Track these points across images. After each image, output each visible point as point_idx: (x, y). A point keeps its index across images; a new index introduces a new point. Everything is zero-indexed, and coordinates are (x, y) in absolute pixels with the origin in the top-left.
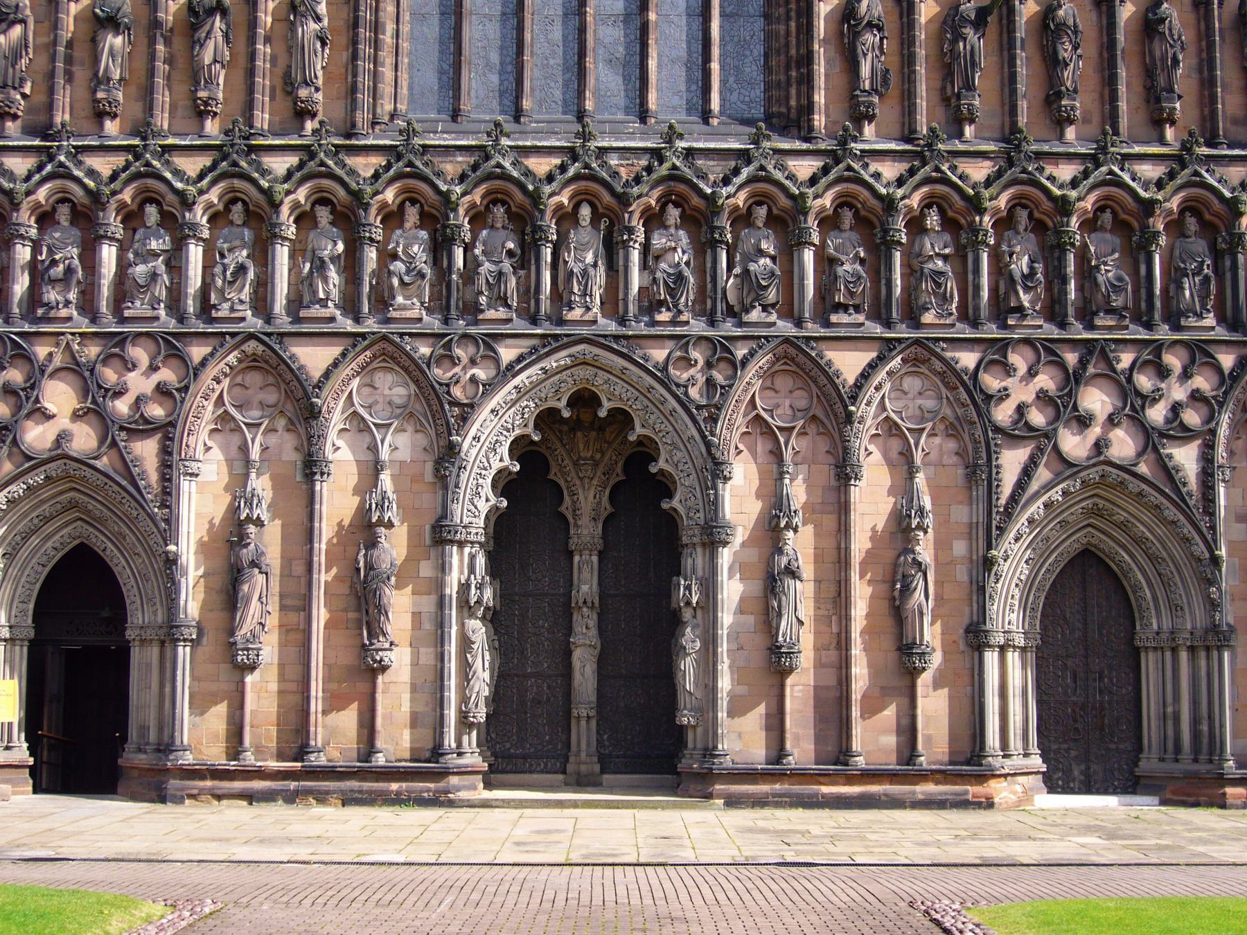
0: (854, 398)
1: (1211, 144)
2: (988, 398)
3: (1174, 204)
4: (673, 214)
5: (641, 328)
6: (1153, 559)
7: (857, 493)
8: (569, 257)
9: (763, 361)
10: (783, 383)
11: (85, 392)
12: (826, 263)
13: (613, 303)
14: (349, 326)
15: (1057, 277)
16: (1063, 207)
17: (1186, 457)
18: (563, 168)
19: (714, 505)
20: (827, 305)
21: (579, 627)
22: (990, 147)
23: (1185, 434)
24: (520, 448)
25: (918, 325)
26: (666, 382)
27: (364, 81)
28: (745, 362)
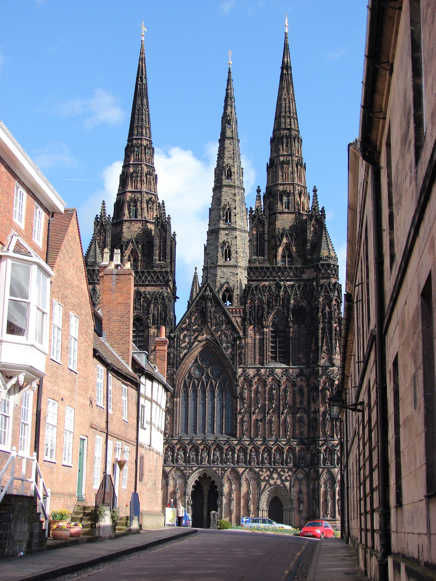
0: (242, 476)
1: (293, 439)
2: (260, 476)
3: (287, 448)
4: (217, 449)
5: (212, 465)
7: (242, 488)
8: (203, 455)
9: (229, 470)
10: (232, 473)
12: (238, 456)
13: (209, 462)
14: (172, 465)
15: (270, 458)
16: (271, 448)
17: (287, 484)
18: (202, 443)
19: (222, 490)
20: (238, 462)
21: (205, 507)
22: (261, 439)
23: (287, 481)
24: (196, 482)
25: (250, 465)
26: (216, 473)
27: (175, 429)
28: (227, 470)
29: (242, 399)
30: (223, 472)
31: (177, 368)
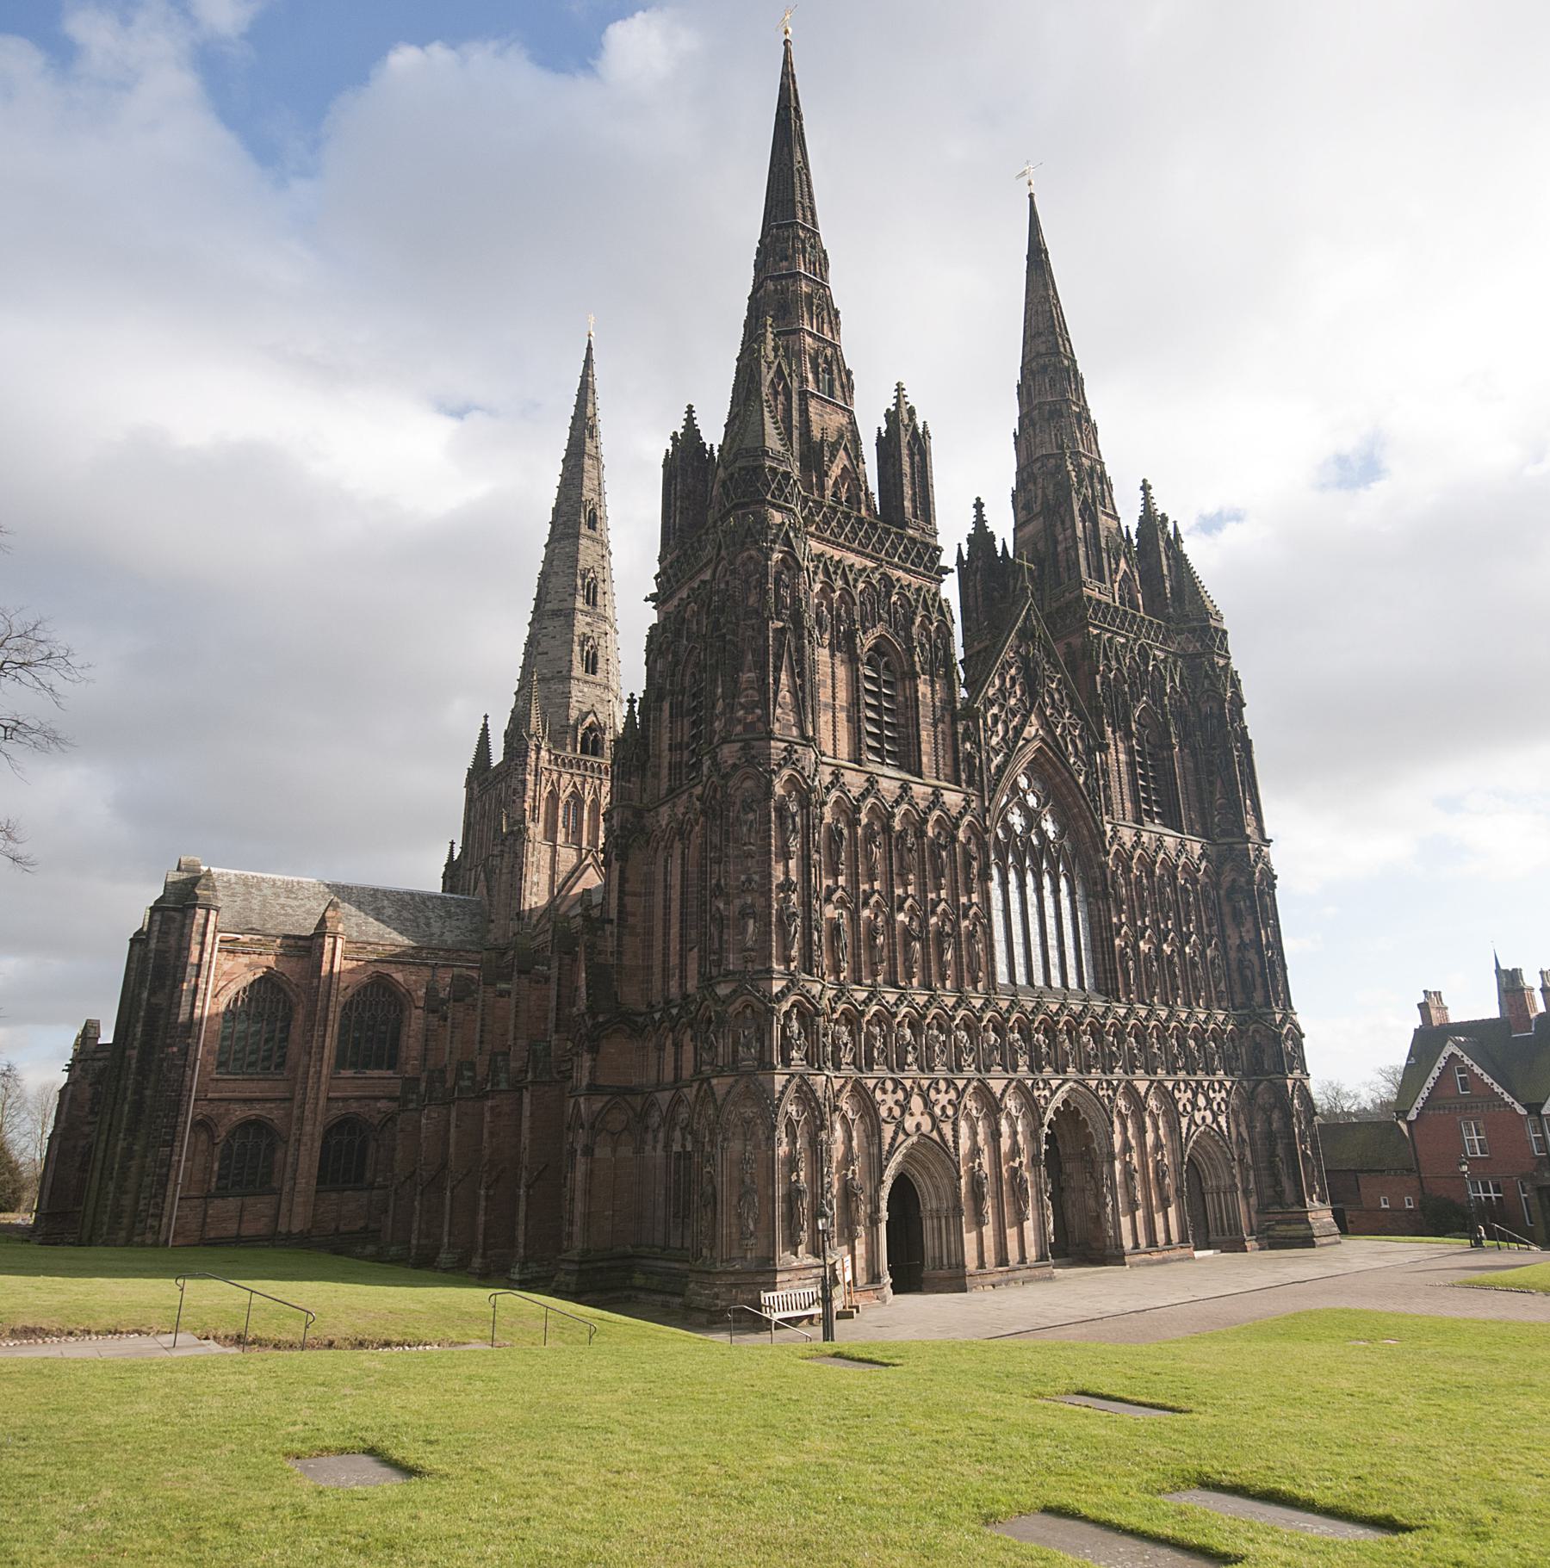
6: (1210, 1158)
11: (926, 1105)
17: (1222, 1120)
26: (1097, 1097)
29: (1119, 903)
30: (1110, 1092)
31: (990, 800)
